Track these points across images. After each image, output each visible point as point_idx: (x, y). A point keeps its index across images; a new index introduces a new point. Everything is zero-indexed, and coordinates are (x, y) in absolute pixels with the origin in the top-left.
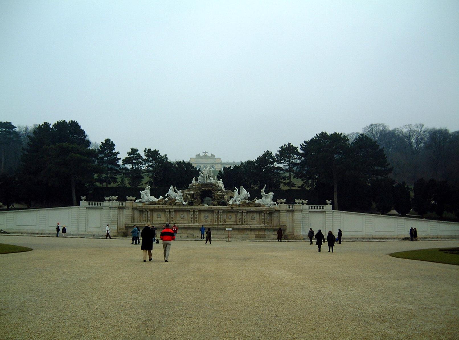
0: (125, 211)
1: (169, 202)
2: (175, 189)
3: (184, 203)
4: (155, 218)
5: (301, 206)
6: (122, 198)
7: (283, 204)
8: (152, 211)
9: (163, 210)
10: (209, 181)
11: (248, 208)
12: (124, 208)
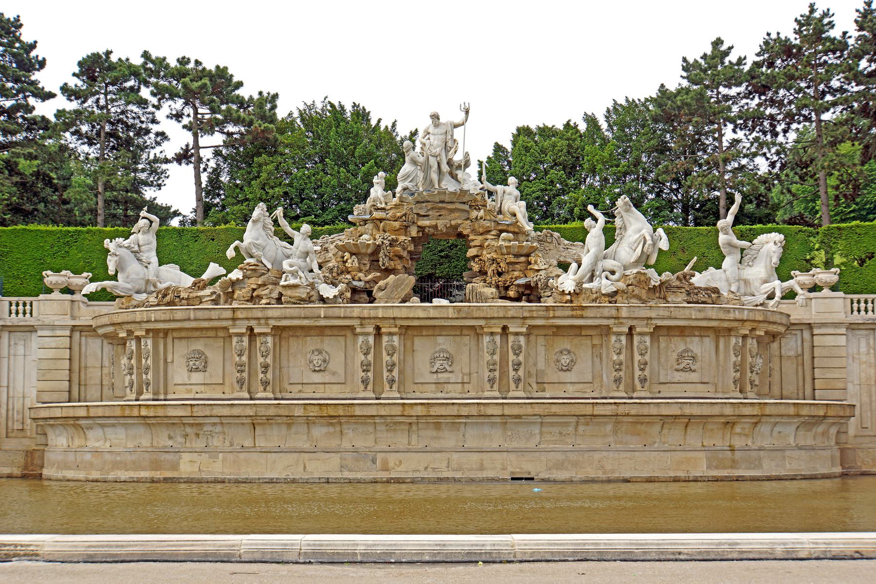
0: (35, 341)
1: (253, 282)
2: (276, 222)
3: (329, 292)
4: (179, 374)
7: (826, 292)
8: (159, 334)
9: (221, 334)
10: (450, 186)
11: (658, 312)
12: (32, 329)
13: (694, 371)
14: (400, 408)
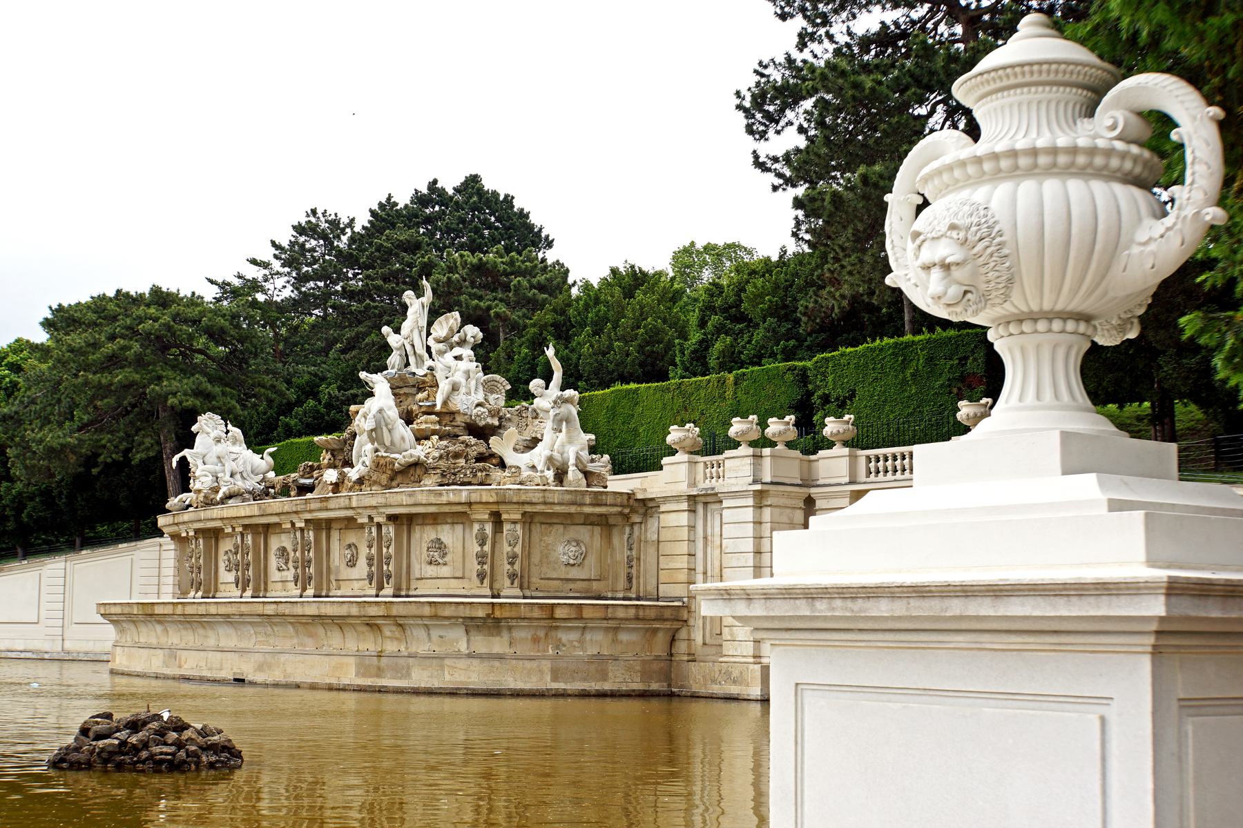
13: (445, 564)
14: (171, 607)
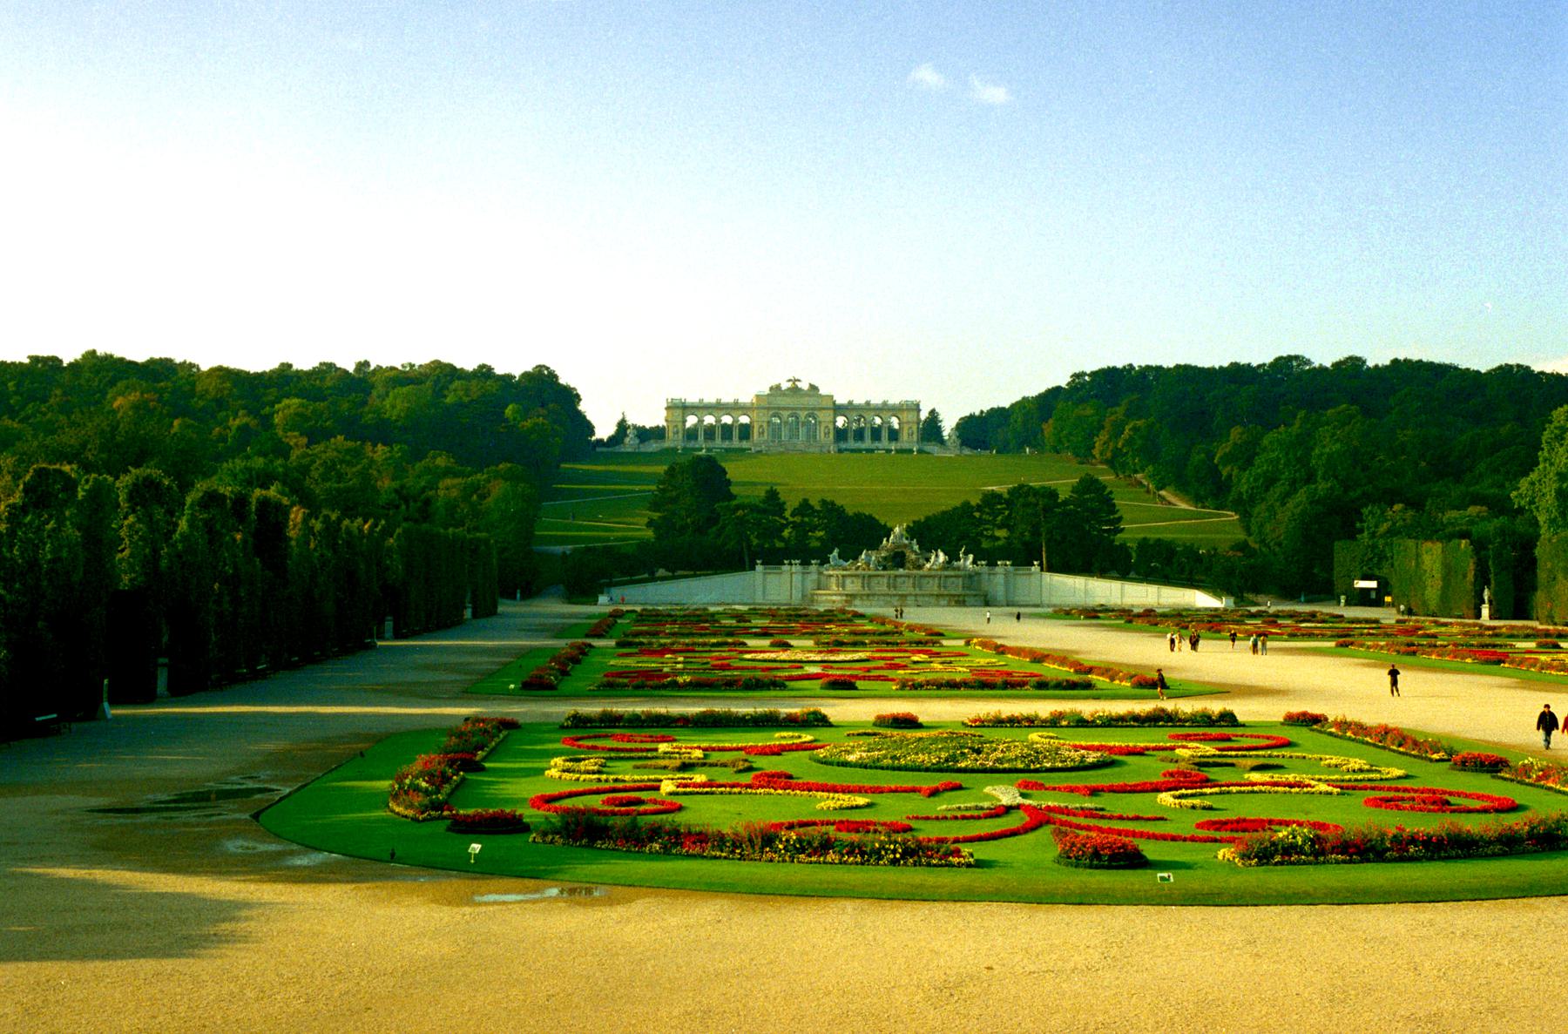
5: (1004, 566)
6: (805, 563)
9: (856, 576)
